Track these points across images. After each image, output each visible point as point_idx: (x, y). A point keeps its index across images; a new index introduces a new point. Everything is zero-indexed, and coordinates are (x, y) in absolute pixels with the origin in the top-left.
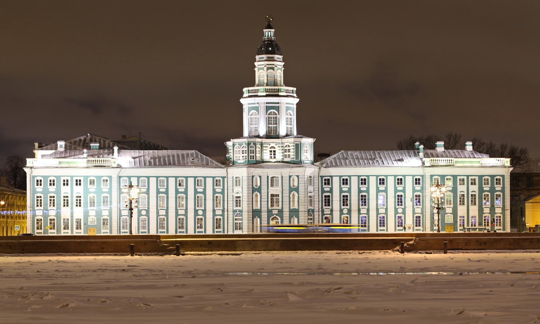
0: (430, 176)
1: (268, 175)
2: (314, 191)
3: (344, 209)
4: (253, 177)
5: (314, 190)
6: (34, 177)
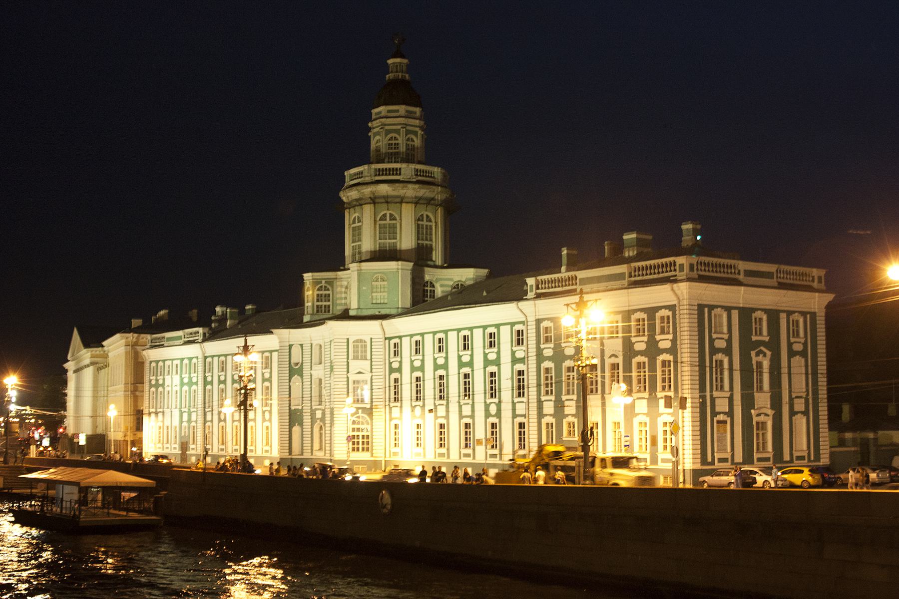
0: (534, 323)
1: (312, 342)
2: (371, 372)
3: (416, 406)
4: (290, 346)
5: (371, 369)
6: (151, 362)
